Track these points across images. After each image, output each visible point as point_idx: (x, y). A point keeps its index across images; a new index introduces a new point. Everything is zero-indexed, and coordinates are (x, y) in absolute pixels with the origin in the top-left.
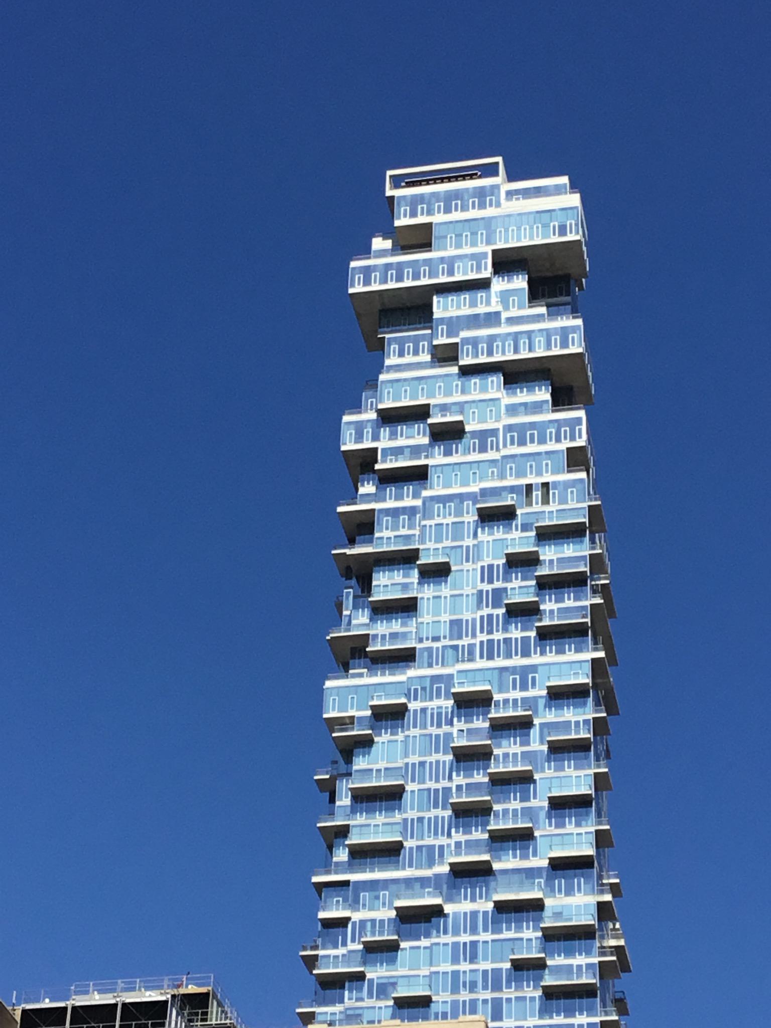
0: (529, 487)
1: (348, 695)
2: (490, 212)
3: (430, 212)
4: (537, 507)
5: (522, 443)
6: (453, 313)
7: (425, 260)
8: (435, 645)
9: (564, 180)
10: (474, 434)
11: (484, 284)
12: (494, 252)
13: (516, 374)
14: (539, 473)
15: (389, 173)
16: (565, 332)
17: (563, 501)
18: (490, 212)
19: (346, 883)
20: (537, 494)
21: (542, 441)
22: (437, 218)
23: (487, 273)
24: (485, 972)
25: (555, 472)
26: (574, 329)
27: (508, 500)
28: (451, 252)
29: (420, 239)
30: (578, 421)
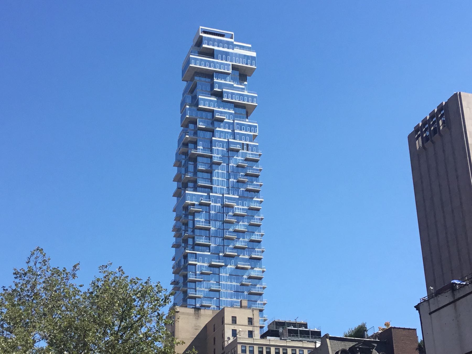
0: (243, 144)
1: (193, 196)
2: (230, 51)
3: (214, 46)
4: (245, 151)
5: (241, 130)
6: (219, 81)
7: (213, 61)
8: (218, 187)
9: (250, 46)
10: (227, 123)
11: (228, 74)
12: (232, 64)
13: (236, 106)
14: (246, 141)
15: (201, 27)
16: (253, 97)
17: (252, 151)
18: (230, 51)
19: (196, 254)
20: (245, 147)
21: (246, 131)
22: (216, 48)
23: (230, 71)
24: (234, 285)
25: (250, 141)
26: (255, 97)
27: (238, 147)
28: (219, 61)
29: (211, 53)
30: (256, 126)
